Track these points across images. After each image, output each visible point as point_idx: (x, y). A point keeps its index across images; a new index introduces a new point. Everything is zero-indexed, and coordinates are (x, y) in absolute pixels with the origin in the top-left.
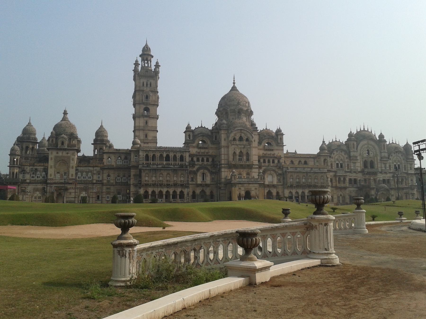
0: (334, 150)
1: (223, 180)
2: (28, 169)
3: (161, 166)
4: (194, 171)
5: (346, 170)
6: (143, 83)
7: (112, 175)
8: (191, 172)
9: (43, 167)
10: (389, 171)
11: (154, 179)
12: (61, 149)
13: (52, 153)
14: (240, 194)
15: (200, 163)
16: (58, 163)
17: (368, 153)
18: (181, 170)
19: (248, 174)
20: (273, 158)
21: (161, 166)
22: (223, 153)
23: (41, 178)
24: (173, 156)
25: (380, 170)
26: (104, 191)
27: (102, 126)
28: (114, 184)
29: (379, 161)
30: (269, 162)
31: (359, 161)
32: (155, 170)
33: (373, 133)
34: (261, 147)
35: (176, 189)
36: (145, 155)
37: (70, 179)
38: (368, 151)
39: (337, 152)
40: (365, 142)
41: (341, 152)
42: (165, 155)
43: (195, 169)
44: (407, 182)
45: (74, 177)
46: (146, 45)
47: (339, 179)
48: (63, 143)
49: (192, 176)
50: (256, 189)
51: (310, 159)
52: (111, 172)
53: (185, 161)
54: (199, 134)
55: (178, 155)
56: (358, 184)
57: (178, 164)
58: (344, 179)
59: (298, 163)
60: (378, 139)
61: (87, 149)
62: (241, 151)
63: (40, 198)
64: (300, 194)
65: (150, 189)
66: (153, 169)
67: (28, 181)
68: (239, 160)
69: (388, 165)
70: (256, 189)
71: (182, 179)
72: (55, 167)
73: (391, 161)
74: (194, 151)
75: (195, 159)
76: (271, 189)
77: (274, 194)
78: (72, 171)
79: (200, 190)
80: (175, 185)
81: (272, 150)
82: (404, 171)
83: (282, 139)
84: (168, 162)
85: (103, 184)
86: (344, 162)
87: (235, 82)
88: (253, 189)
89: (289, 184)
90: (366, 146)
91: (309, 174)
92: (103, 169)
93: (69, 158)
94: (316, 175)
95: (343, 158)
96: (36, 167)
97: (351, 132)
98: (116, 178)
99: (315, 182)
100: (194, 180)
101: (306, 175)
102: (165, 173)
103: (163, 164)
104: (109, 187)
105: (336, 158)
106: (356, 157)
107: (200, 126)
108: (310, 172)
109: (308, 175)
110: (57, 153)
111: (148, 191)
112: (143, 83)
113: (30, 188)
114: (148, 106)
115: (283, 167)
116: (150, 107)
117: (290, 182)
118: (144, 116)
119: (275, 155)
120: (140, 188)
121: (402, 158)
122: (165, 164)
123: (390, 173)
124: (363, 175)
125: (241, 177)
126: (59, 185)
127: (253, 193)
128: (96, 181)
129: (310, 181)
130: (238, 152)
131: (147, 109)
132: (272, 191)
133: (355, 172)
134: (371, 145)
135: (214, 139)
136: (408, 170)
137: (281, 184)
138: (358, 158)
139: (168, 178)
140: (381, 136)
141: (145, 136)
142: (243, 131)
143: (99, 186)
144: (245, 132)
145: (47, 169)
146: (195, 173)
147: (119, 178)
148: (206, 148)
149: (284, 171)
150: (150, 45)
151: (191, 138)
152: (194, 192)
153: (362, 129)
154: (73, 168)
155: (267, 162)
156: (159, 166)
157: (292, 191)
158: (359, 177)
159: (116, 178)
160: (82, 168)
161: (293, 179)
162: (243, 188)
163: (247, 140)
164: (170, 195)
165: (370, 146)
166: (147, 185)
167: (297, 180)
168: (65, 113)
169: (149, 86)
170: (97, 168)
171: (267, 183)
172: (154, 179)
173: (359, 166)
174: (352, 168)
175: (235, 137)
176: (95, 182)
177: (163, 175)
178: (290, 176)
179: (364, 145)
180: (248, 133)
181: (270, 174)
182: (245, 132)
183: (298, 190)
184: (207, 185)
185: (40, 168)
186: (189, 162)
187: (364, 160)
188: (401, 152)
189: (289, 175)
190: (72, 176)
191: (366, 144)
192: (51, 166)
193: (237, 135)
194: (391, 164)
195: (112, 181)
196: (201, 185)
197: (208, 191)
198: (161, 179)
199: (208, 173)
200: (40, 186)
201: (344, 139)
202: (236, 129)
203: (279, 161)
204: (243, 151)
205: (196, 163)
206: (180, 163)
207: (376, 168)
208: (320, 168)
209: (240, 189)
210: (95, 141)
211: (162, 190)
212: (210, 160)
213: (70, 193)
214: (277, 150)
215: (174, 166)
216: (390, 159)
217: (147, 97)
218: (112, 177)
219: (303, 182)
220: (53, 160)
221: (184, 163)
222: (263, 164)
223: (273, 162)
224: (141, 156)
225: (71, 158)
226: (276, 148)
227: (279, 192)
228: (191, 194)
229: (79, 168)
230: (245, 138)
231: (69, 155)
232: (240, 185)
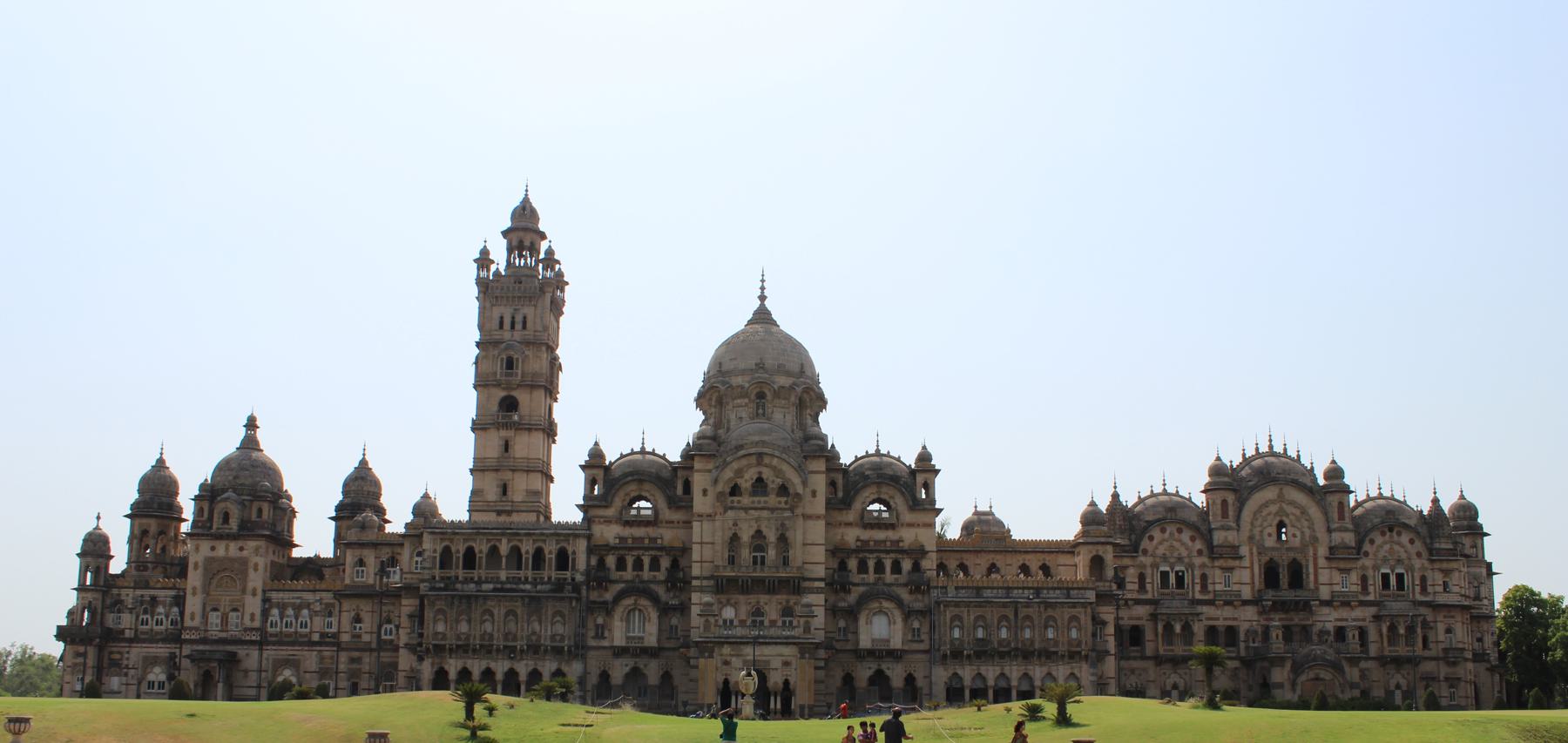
0: (1150, 524)
1: (695, 636)
2: (129, 596)
3: (491, 586)
4: (605, 603)
5: (1198, 596)
7: (366, 617)
8: (593, 607)
9: (173, 593)
10: (1362, 598)
11: (463, 627)
12: (219, 537)
13: (197, 549)
14: (726, 682)
15: (629, 574)
16: (215, 582)
18: (554, 598)
19: (787, 612)
21: (491, 586)
22: (696, 538)
23: (167, 625)
24: (531, 551)
25: (1325, 593)
26: (342, 667)
28: (374, 646)
29: (1322, 562)
30: (879, 567)
31: (1246, 563)
32: (469, 597)
33: (1306, 462)
34: (851, 516)
35: (540, 663)
36: (439, 548)
37: (246, 630)
38: (1281, 525)
39: (1163, 531)
40: (1270, 493)
41: (1180, 531)
42: (504, 548)
43: (608, 596)
44: (1431, 638)
45: (257, 624)
47: (1168, 628)
48: (226, 518)
49: (600, 621)
50: (786, 664)
51: (1063, 559)
52: (365, 607)
54: (626, 475)
55: (550, 550)
56: (1242, 645)
58: (1187, 628)
59: (984, 569)
60: (1321, 482)
61: (314, 536)
62: (759, 533)
63: (161, 685)
64: (991, 682)
65: (452, 661)
66: (461, 597)
67: (128, 634)
68: (755, 563)
69: (1354, 577)
70: (786, 664)
71: (559, 629)
72: (207, 592)
73: (1368, 562)
74: (609, 533)
75: (611, 561)
76: (884, 667)
77: (897, 681)
78: (253, 605)
79: (627, 669)
80: (534, 649)
81: (892, 526)
82: (1419, 597)
83: (928, 487)
84: (514, 573)
85: (339, 646)
86: (1191, 566)
88: (776, 663)
89: (946, 649)
90: (1273, 508)
91: (1023, 612)
92: (341, 595)
93: (244, 562)
94: (1050, 612)
95: (1184, 553)
96: (152, 592)
97: (1218, 459)
98: (380, 627)
101: (1012, 617)
102: (499, 612)
103: (498, 580)
104: (356, 654)
105: (1161, 551)
106: (1235, 548)
108: (1028, 605)
109: (1021, 616)
110: (213, 548)
113: (135, 654)
114: (515, 394)
116: (522, 396)
117: (952, 640)
118: (499, 426)
119: (905, 545)
120: (421, 659)
121: (1413, 550)
123: (1362, 604)
124: (1260, 613)
125: (762, 622)
126: (201, 647)
127: (775, 680)
128: (323, 635)
129: (1027, 634)
130: (746, 536)
132: (888, 673)
133: (1228, 603)
134: (1292, 503)
135: (680, 491)
137: (922, 647)
138: (1244, 551)
139: (512, 626)
140: (1335, 473)
141: (500, 490)
143: (328, 652)
144: (775, 461)
145: (184, 597)
146: (607, 609)
147: (389, 626)
150: (536, 203)
152: (605, 676)
154: (254, 594)
155: (871, 569)
156: (485, 587)
157: (960, 672)
158: (1247, 618)
159: (380, 627)
160: (281, 595)
161: (961, 628)
163: (783, 490)
165: (1289, 509)
167: (980, 634)
168: (251, 424)
170: (324, 594)
171: (865, 642)
172: (463, 627)
173: (1246, 579)
174: (1218, 587)
175: (739, 481)
176: (316, 637)
177: (492, 615)
178: (952, 621)
179: (1266, 505)
180: (785, 467)
181: (880, 611)
182: (775, 461)
183: (983, 670)
185: (164, 595)
186: (587, 573)
187: (1265, 559)
188: (1406, 526)
190: (252, 619)
191: (1273, 502)
192: (194, 589)
193: (747, 476)
194: (1370, 573)
195: (366, 638)
197: (653, 672)
198: (488, 627)
200: (162, 650)
201: (1193, 487)
202: (742, 453)
203: (916, 567)
204: (765, 531)
205: (615, 575)
207: (1312, 586)
208: (1068, 589)
210: (340, 508)
211: (493, 665)
212: (665, 563)
213: (246, 671)
214: (910, 525)
215: (534, 583)
216: (1366, 554)
217: (510, 364)
218: (367, 625)
219: (1001, 642)
220: (200, 570)
221: (568, 574)
222: (856, 578)
223: (897, 568)
224: (426, 554)
225: (251, 565)
226: (908, 517)
228: (593, 679)
229: (274, 595)
230: (773, 483)
231: (245, 553)
232: (726, 650)
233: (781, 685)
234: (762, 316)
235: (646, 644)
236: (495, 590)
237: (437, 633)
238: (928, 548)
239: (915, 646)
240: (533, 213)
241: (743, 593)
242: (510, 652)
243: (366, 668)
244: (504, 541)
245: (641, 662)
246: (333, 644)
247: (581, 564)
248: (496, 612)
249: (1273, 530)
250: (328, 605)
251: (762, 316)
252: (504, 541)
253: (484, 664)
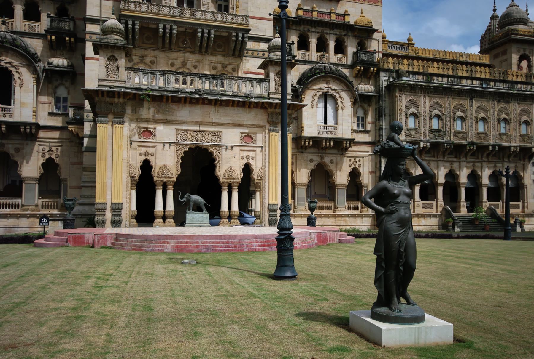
14: (146, 166)
20: (337, 32)
76: (327, 160)
77: (342, 178)
99: (500, 135)
115: (379, 71)
117: (408, 130)
127: (229, 165)
137: (367, 138)
149: (385, 84)
162: (165, 133)
167: (435, 124)
178: (408, 107)
189: (403, 100)
199: (23, 70)
203: (362, 47)
209: (149, 133)
219: (457, 133)
227: (361, 170)
232: (147, 111)
233: (238, 174)
235: (16, 118)
238: (374, 27)
239: (359, 137)
241: (163, 49)
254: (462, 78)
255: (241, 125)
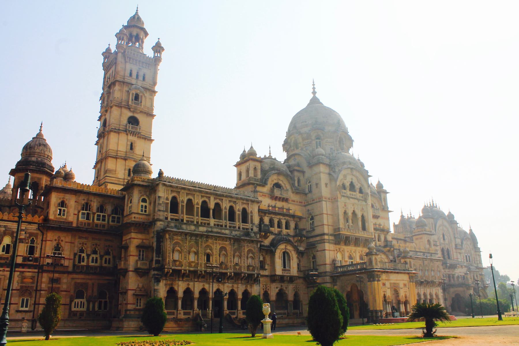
6: (131, 71)
11: (192, 258)
17: (444, 239)
27: (39, 136)
28: (70, 269)
29: (454, 249)
46: (137, 13)
52: (66, 239)
53: (252, 223)
57: (239, 228)
65: (180, 283)
70: (405, 285)
74: (266, 202)
75: (266, 220)
87: (316, 90)
100: (267, 267)
104: (56, 275)
107: (267, 156)
111: (176, 288)
112: (131, 71)
114: (136, 115)
122: (212, 224)
131: (133, 121)
135: (296, 185)
136: (477, 264)
139: (222, 259)
142: (355, 173)
143: (29, 273)
148: (286, 200)
151: (259, 176)
153: (431, 203)
156: (202, 229)
159: (75, 254)
164: (208, 299)
166: (178, 274)
169: (141, 78)
172: (192, 258)
176: (19, 260)
177: (211, 250)
184: (292, 279)
195: (66, 263)
196: (282, 279)
206: (242, 225)
211: (206, 286)
221: (248, 226)
224: (162, 200)
230: (357, 186)
234: (315, 101)
236: (207, 231)
237: (175, 261)
240: (139, 19)
242: (221, 277)
243: (64, 287)
244: (212, 198)
245: (284, 285)
246: (35, 267)
247: (256, 220)
248: (214, 247)
249: (442, 236)
250: (31, 234)
251: (315, 101)
252: (212, 198)
253: (215, 287)
254: (417, 252)
255: (403, 280)
